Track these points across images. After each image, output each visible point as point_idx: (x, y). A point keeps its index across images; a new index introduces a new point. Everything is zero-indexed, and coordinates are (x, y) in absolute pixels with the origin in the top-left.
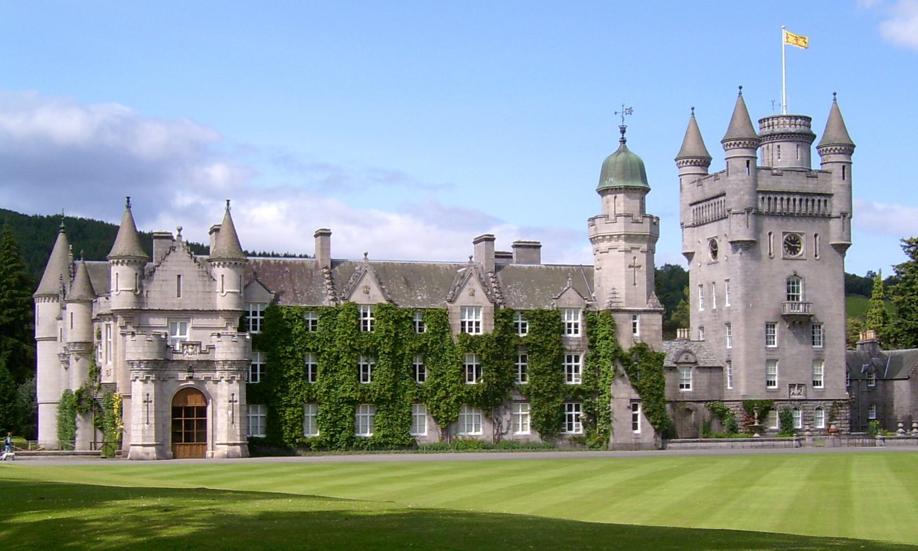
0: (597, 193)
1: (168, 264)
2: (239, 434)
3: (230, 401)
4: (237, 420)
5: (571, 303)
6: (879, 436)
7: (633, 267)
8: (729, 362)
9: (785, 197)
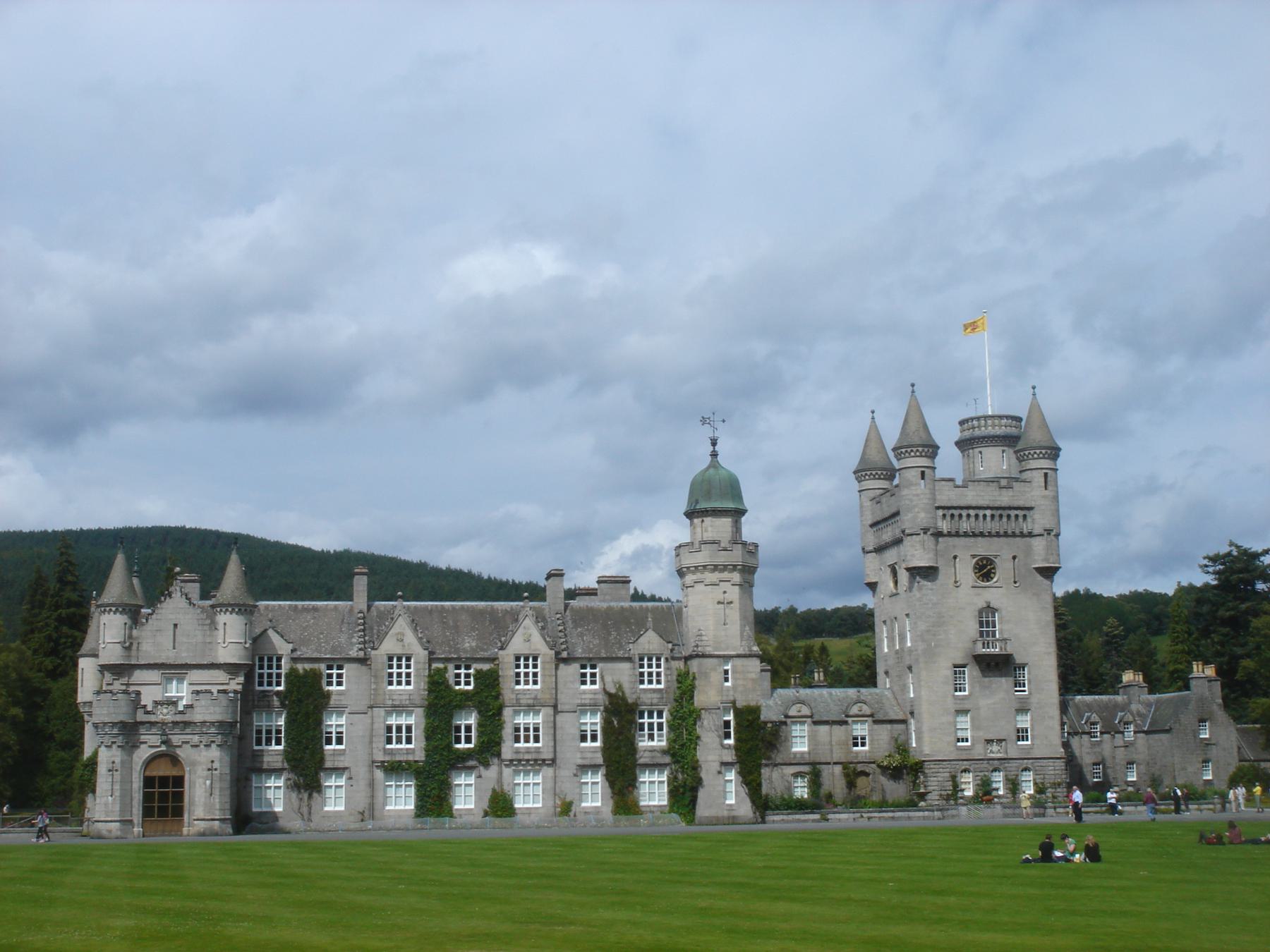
0: (685, 517)
1: (164, 611)
2: (218, 807)
3: (209, 770)
4: (217, 792)
5: (651, 648)
7: (723, 603)
8: (912, 713)
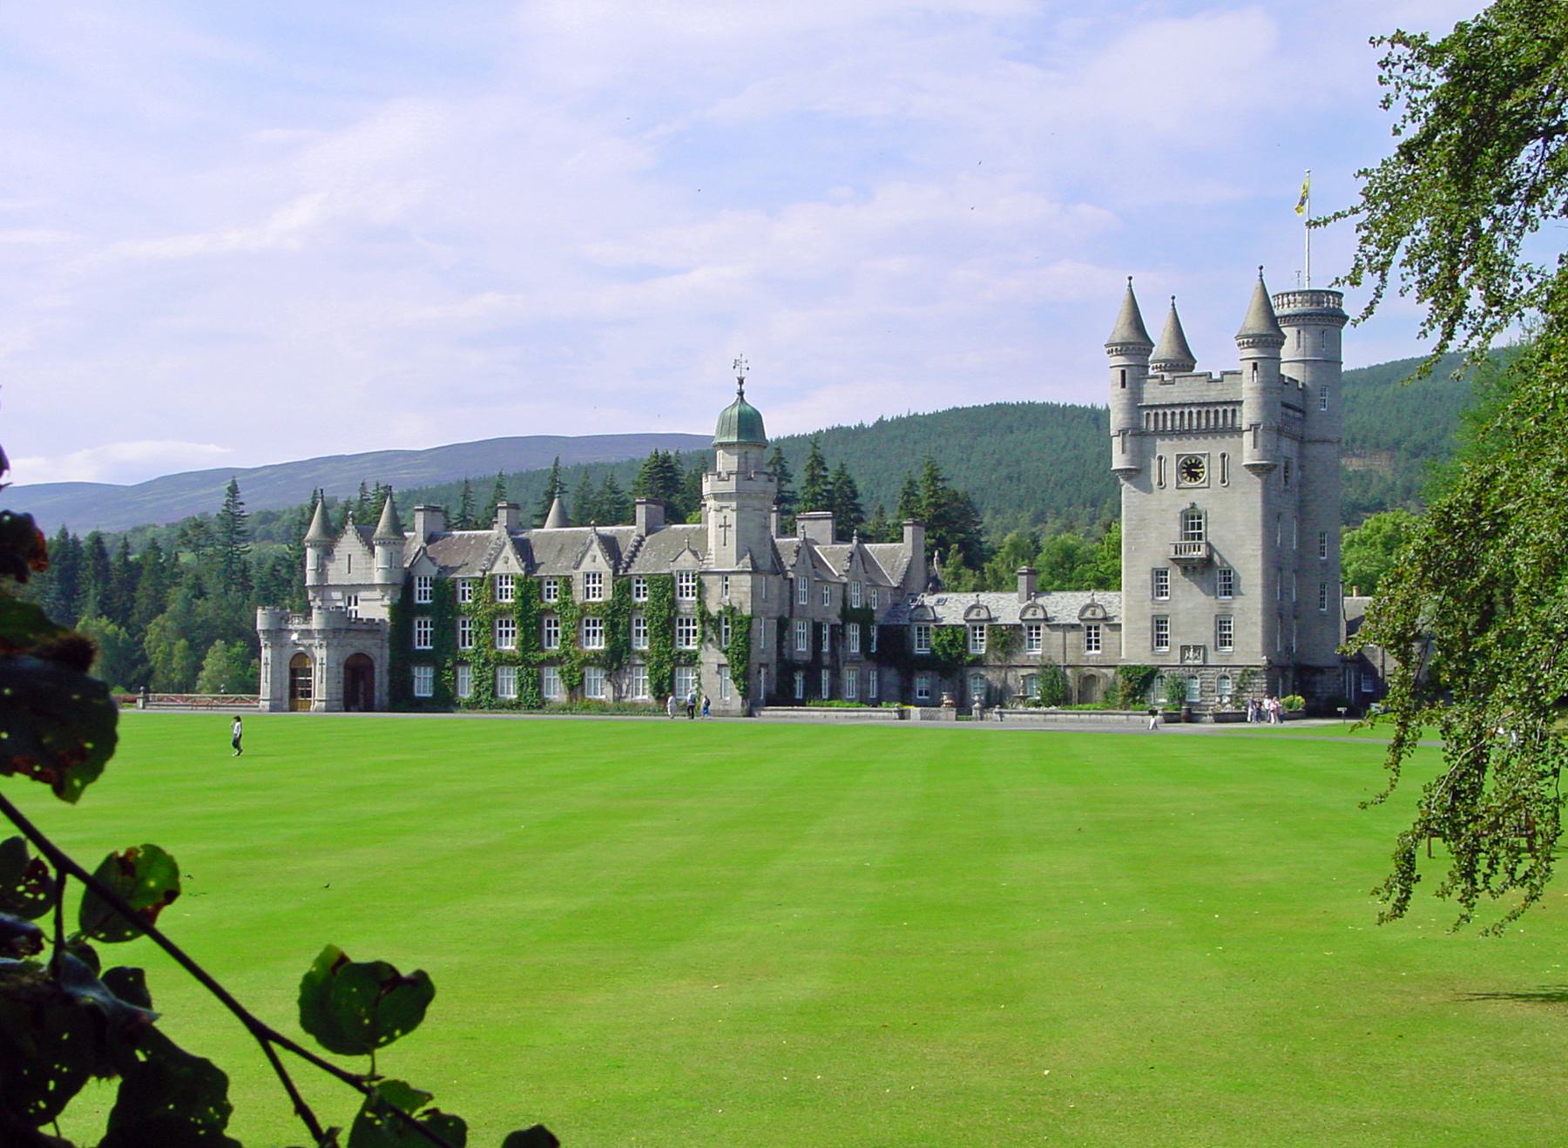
6: (997, 710)
9: (1178, 411)
